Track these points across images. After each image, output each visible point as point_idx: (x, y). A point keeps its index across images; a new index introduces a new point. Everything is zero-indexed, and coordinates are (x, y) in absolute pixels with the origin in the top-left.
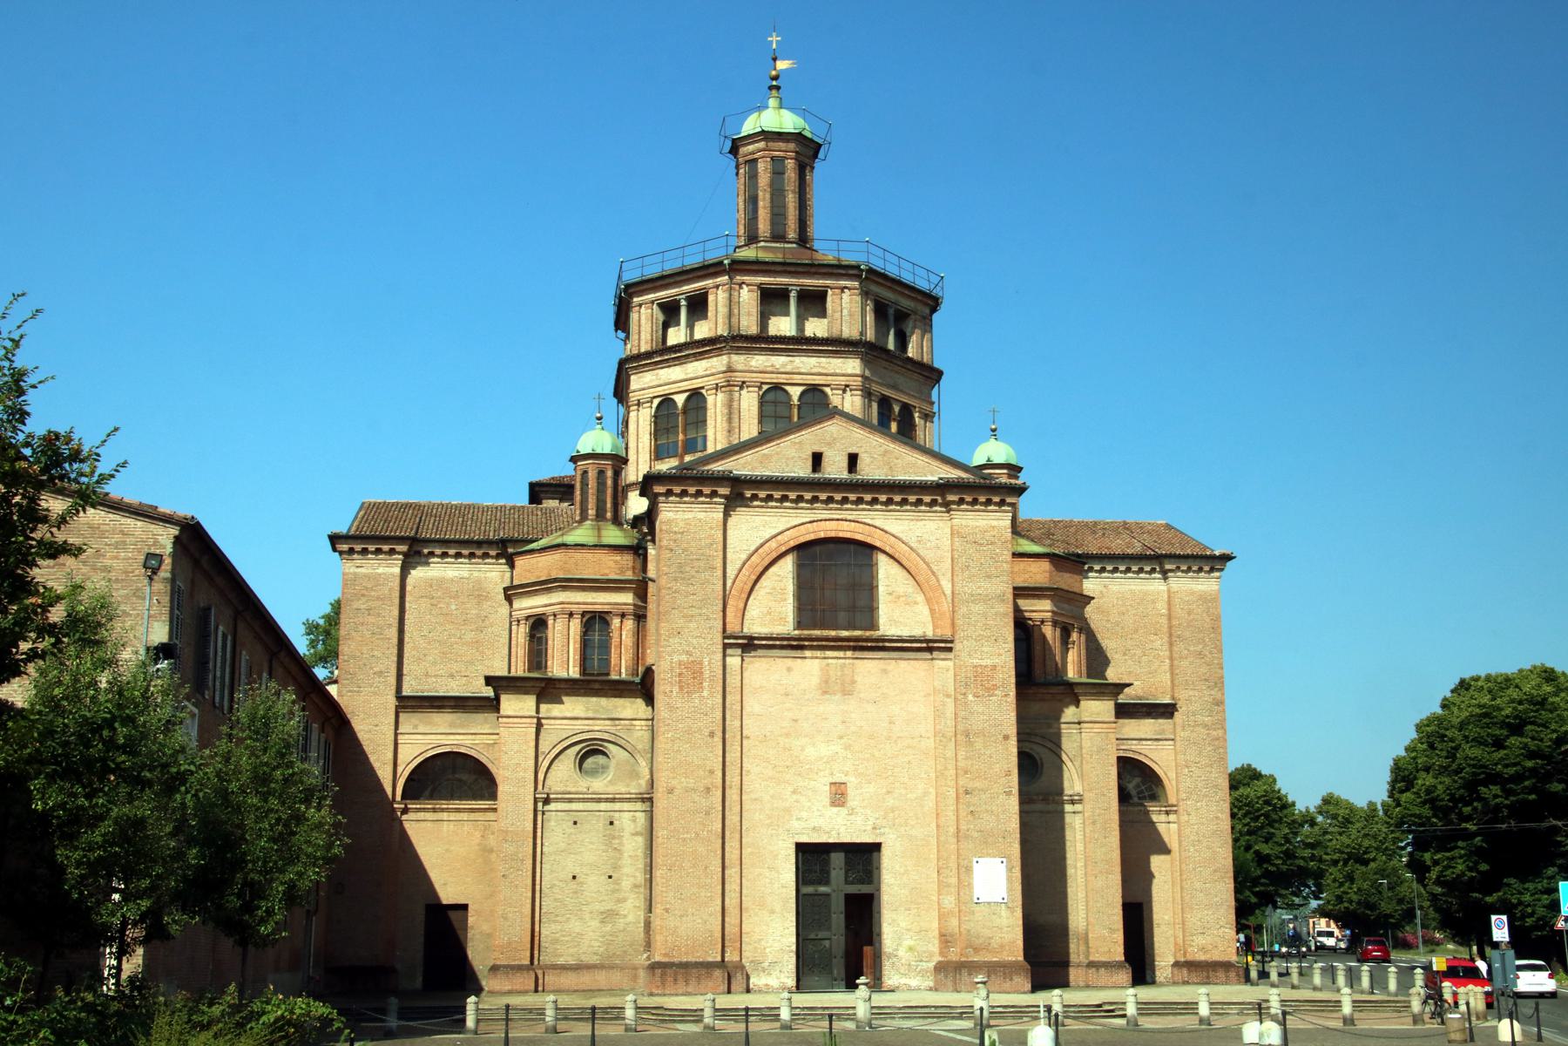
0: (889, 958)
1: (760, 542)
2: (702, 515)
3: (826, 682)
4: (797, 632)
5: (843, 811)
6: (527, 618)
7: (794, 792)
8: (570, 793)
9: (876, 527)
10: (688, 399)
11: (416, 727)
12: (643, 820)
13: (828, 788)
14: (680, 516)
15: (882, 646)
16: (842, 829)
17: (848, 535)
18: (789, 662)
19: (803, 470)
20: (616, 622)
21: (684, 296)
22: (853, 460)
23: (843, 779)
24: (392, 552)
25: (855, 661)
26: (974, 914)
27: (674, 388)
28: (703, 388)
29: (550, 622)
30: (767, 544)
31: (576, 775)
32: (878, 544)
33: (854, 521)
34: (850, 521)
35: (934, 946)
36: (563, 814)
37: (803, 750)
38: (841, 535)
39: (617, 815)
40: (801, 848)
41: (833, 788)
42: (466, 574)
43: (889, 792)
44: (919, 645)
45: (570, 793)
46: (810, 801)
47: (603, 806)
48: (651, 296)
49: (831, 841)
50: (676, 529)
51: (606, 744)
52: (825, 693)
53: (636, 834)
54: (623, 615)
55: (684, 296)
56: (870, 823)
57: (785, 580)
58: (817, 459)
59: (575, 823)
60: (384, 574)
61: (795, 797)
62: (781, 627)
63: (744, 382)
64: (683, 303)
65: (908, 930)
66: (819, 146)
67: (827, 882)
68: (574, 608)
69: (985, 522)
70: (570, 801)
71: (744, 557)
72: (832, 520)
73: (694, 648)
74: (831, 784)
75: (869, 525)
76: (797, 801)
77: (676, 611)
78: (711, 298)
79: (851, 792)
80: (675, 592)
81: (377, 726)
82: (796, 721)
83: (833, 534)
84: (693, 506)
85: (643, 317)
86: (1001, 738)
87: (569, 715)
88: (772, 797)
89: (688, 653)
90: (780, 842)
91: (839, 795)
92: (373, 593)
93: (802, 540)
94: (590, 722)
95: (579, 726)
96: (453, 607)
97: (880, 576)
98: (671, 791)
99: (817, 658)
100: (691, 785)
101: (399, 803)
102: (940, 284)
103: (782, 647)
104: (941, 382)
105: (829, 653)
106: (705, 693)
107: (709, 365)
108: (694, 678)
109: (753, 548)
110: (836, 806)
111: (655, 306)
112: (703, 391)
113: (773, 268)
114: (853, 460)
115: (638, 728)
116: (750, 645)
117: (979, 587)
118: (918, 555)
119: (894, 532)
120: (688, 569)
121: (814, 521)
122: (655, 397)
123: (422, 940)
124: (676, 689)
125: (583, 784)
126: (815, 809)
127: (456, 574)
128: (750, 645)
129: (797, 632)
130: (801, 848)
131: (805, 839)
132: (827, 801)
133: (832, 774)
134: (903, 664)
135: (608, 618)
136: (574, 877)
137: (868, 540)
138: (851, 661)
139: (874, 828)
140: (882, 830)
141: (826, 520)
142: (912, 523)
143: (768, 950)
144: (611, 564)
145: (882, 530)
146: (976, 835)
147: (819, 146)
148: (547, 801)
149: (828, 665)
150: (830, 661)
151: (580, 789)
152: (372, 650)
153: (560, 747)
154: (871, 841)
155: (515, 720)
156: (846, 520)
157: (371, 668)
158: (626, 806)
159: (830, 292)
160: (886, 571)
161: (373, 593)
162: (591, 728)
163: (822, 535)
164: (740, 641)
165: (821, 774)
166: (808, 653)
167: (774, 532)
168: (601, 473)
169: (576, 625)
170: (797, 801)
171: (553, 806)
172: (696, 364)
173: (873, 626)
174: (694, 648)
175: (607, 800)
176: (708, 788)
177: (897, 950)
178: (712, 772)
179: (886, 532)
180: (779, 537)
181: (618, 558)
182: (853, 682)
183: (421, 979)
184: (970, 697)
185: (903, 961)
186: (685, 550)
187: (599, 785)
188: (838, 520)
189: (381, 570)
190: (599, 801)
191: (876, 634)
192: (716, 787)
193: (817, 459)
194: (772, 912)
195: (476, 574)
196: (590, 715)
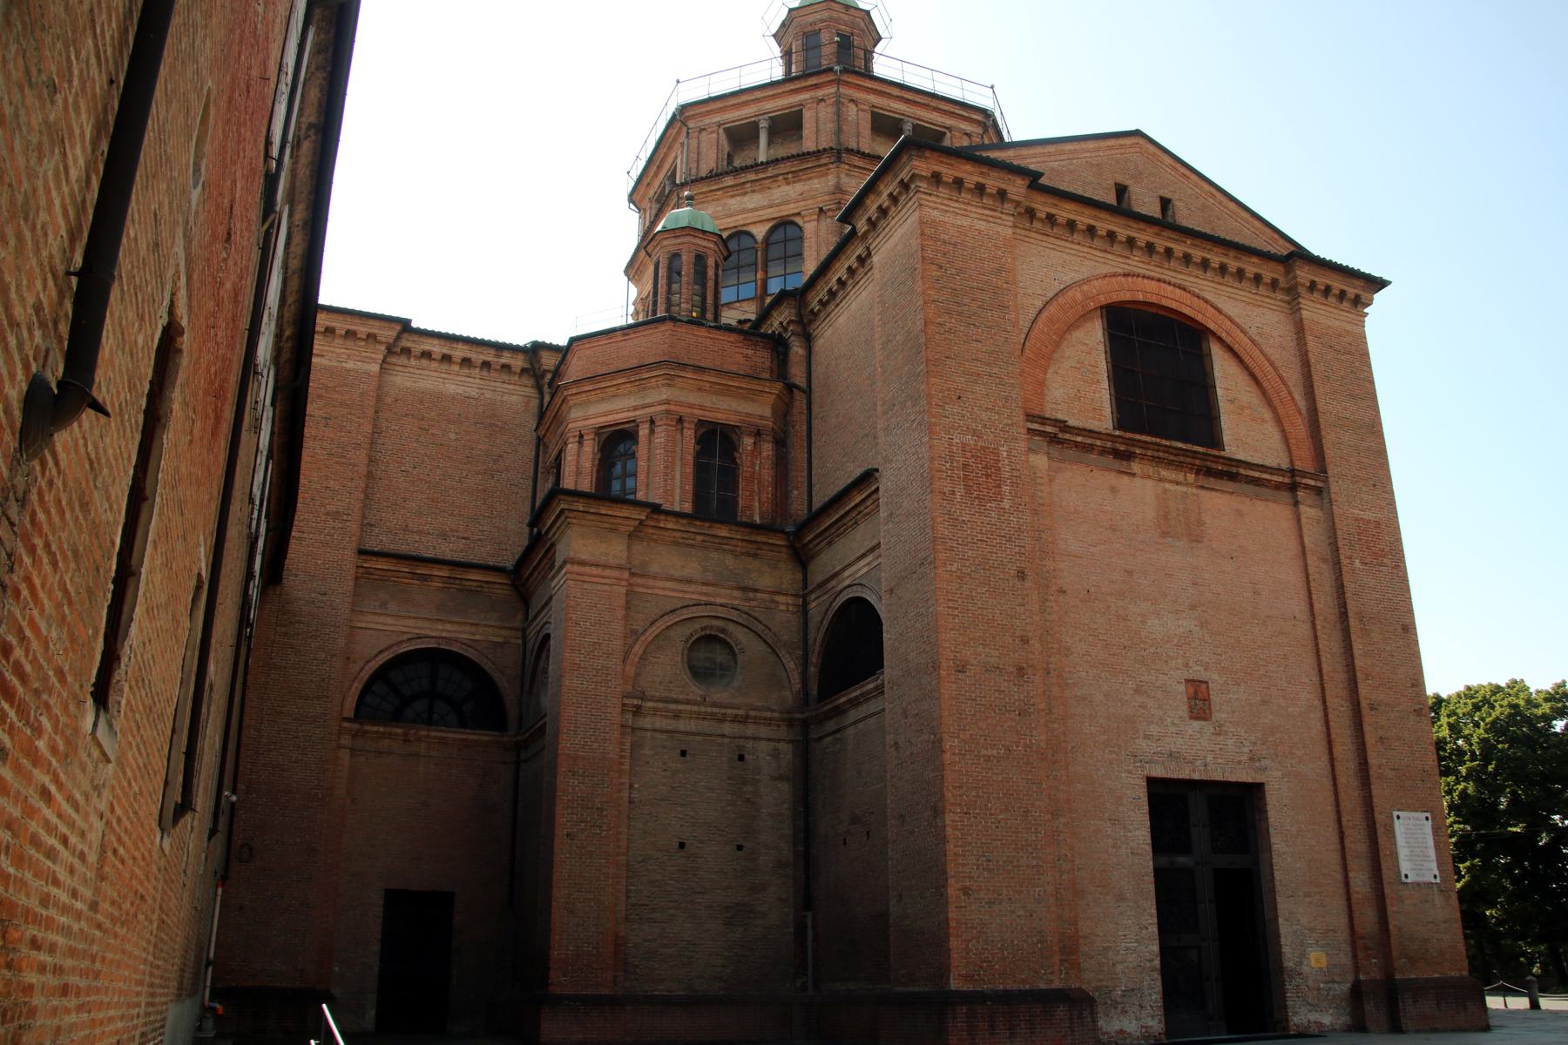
0: (1291, 977)
1: (1058, 287)
2: (982, 225)
3: (1166, 517)
4: (1117, 433)
5: (1208, 727)
6: (599, 430)
7: (1137, 691)
8: (676, 701)
11: (384, 604)
12: (789, 757)
13: (1182, 688)
14: (949, 218)
16: (1209, 758)
17: (1174, 305)
18: (1112, 479)
20: (748, 442)
21: (766, 116)
23: (1203, 676)
24: (371, 337)
25: (1203, 493)
26: (1403, 902)
27: (750, 217)
28: (799, 214)
29: (643, 431)
30: (1070, 293)
31: (686, 676)
32: (1212, 326)
33: (1179, 287)
34: (1174, 285)
35: (1345, 959)
36: (664, 736)
37: (1144, 622)
38: (1164, 302)
39: (749, 744)
40: (1151, 781)
41: (1191, 690)
42: (474, 393)
43: (1264, 702)
44: (1280, 479)
45: (676, 701)
46: (1160, 707)
47: (727, 728)
48: (717, 118)
49: (1196, 776)
50: (946, 237)
51: (731, 627)
52: (1165, 534)
53: (780, 778)
54: (758, 434)
55: (766, 116)
56: (1246, 750)
57: (1094, 352)
59: (683, 753)
60: (354, 370)
61: (1139, 699)
62: (1096, 423)
64: (763, 124)
65: (1312, 930)
67: (1186, 849)
68: (684, 411)
69: (1338, 323)
70: (677, 716)
71: (1039, 304)
72: (1152, 279)
73: (985, 426)
74: (1187, 681)
76: (1143, 706)
77: (948, 362)
79: (1215, 699)
80: (949, 331)
81: (325, 594)
82: (1130, 573)
83: (1154, 299)
84: (969, 208)
85: (703, 145)
86: (1400, 630)
87: (677, 574)
88: (1105, 695)
89: (975, 433)
90: (1123, 775)
91: (1199, 702)
92: (336, 396)
93: (1115, 298)
94: (710, 589)
95: (693, 593)
96: (453, 436)
97: (1216, 374)
98: (961, 668)
99: (1149, 477)
100: (993, 661)
101: (347, 720)
103: (1103, 452)
105: (1164, 473)
106: (1006, 504)
107: (807, 188)
108: (988, 476)
109: (1051, 295)
110: (1197, 719)
111: (721, 131)
112: (798, 220)
113: (888, 90)
115: (783, 607)
117: (1345, 409)
118: (1262, 352)
119: (1230, 313)
120: (967, 301)
121: (1129, 275)
123: (376, 948)
124: (960, 491)
125: (695, 690)
126: (1169, 720)
127: (460, 390)
129: (1117, 433)
130: (1151, 781)
131: (1159, 772)
132: (1183, 711)
133: (1187, 665)
134: (1260, 506)
135: (734, 437)
136: (682, 845)
137: (1199, 318)
138: (1194, 490)
139: (1251, 759)
140: (1264, 763)
141: (1144, 277)
142: (1249, 307)
143: (1119, 968)
144: (742, 360)
145: (1216, 308)
146: (1390, 774)
148: (637, 711)
149: (1165, 491)
150: (1167, 486)
151: (691, 697)
152: (327, 478)
153: (661, 625)
155: (594, 571)
156: (1169, 284)
157: (322, 505)
158: (764, 731)
159: (948, 135)
161: (336, 396)
162: (712, 600)
163: (1141, 297)
164: (1049, 429)
165: (1173, 664)
166: (1136, 467)
167: (1077, 277)
168: (700, 259)
169: (689, 439)
170: (1143, 706)
171: (646, 722)
172: (787, 188)
173: (1220, 446)
174: (985, 426)
175: (735, 720)
176: (1020, 669)
177: (1301, 963)
178: (1025, 640)
179: (1220, 311)
180: (1085, 288)
181: (750, 352)
182: (1201, 523)
183: (373, 1013)
185: (1310, 983)
186: (960, 271)
187: (719, 694)
188: (1159, 280)
189: (350, 365)
190: (722, 720)
191: (1222, 453)
192: (1032, 666)
194: (1121, 898)
195: (488, 395)
196: (710, 577)
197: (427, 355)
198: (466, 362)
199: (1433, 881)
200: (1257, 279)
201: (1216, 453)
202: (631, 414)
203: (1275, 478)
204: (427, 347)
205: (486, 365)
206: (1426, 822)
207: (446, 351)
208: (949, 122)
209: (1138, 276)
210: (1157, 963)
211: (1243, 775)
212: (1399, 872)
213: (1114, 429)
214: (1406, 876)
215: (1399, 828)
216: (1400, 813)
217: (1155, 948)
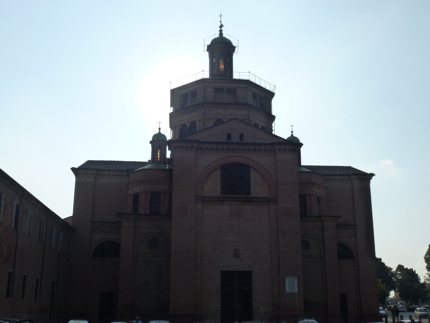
4: (221, 196)
9: (250, 159)
10: (191, 125)
15: (252, 201)
19: (224, 139)
20: (162, 195)
22: (241, 136)
29: (140, 195)
32: (250, 165)
40: (222, 272)
44: (265, 200)
49: (234, 270)
58: (229, 136)
59: (147, 264)
63: (208, 118)
66: (235, 47)
74: (234, 249)
75: (247, 158)
78: (198, 92)
102: (274, 89)
104: (275, 121)
114: (241, 136)
116: (205, 200)
122: (181, 125)
128: (205, 200)
130: (222, 272)
131: (224, 269)
136: (146, 283)
147: (235, 47)
154: (248, 270)
156: (239, 157)
160: (253, 175)
163: (231, 162)
173: (249, 193)
184: (284, 218)
188: (236, 156)
193: (229, 136)
197: (104, 175)
198: (113, 175)
199: (296, 292)
200: (265, 150)
201: (248, 196)
202: (138, 191)
203: (264, 200)
204: (104, 173)
205: (118, 175)
206: (295, 279)
207: (108, 173)
208: (237, 85)
209: (230, 157)
210: (220, 309)
211: (247, 269)
212: (286, 290)
213: (221, 195)
214: (287, 291)
215: (287, 281)
216: (287, 277)
217: (220, 306)
